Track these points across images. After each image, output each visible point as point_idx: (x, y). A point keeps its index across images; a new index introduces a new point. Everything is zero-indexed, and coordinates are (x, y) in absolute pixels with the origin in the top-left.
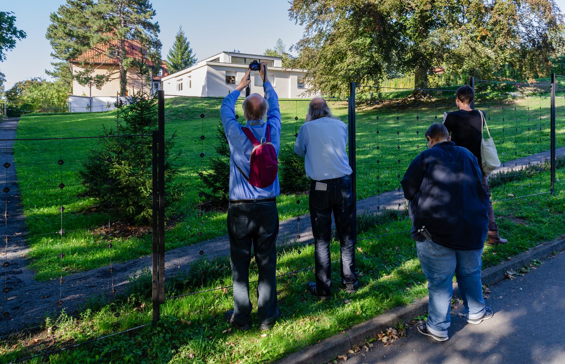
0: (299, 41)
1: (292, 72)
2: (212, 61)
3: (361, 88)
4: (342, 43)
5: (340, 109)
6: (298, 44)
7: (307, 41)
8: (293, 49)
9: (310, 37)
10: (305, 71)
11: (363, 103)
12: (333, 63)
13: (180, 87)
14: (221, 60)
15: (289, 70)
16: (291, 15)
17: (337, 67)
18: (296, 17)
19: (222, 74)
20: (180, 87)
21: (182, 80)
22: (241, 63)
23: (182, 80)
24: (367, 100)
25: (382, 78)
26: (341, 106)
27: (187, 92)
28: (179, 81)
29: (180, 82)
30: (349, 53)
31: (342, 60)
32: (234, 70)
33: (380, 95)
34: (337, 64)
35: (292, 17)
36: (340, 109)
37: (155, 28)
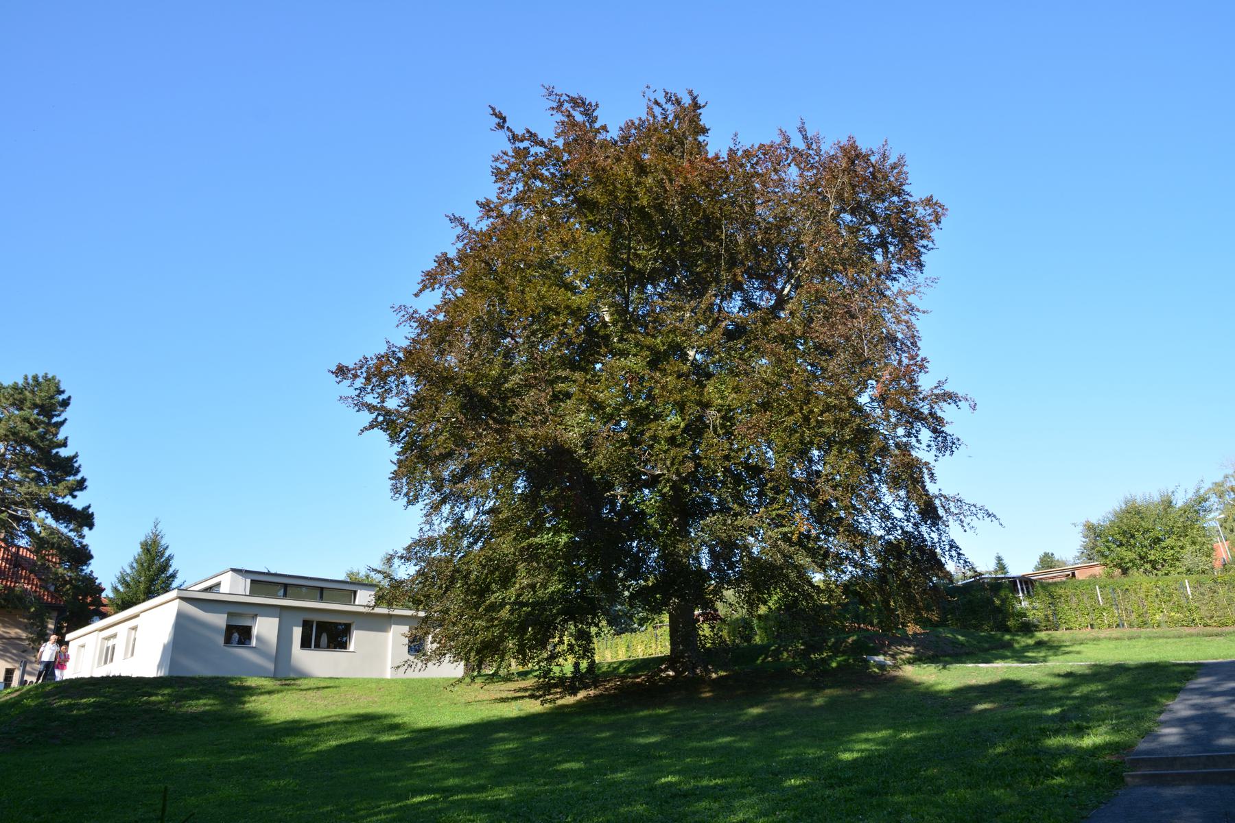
0: (409, 542)
1: (390, 616)
2: (206, 590)
3: (549, 647)
4: (506, 545)
5: (503, 700)
6: (408, 549)
7: (430, 543)
8: (396, 561)
9: (436, 535)
10: (422, 614)
11: (555, 686)
12: (484, 591)
13: (108, 655)
14: (224, 589)
15: (384, 611)
16: (396, 490)
17: (492, 599)
18: (407, 494)
19: (219, 620)
20: (108, 655)
21: (114, 636)
22: (275, 596)
23: (114, 636)
24: (562, 680)
25: (597, 625)
26: (504, 695)
27: (123, 667)
28: (108, 639)
29: (110, 643)
30: (521, 567)
31: (506, 582)
32: (253, 611)
33: (592, 665)
34: (494, 592)
35: (399, 492)
36: (503, 700)
37: (85, 519)
